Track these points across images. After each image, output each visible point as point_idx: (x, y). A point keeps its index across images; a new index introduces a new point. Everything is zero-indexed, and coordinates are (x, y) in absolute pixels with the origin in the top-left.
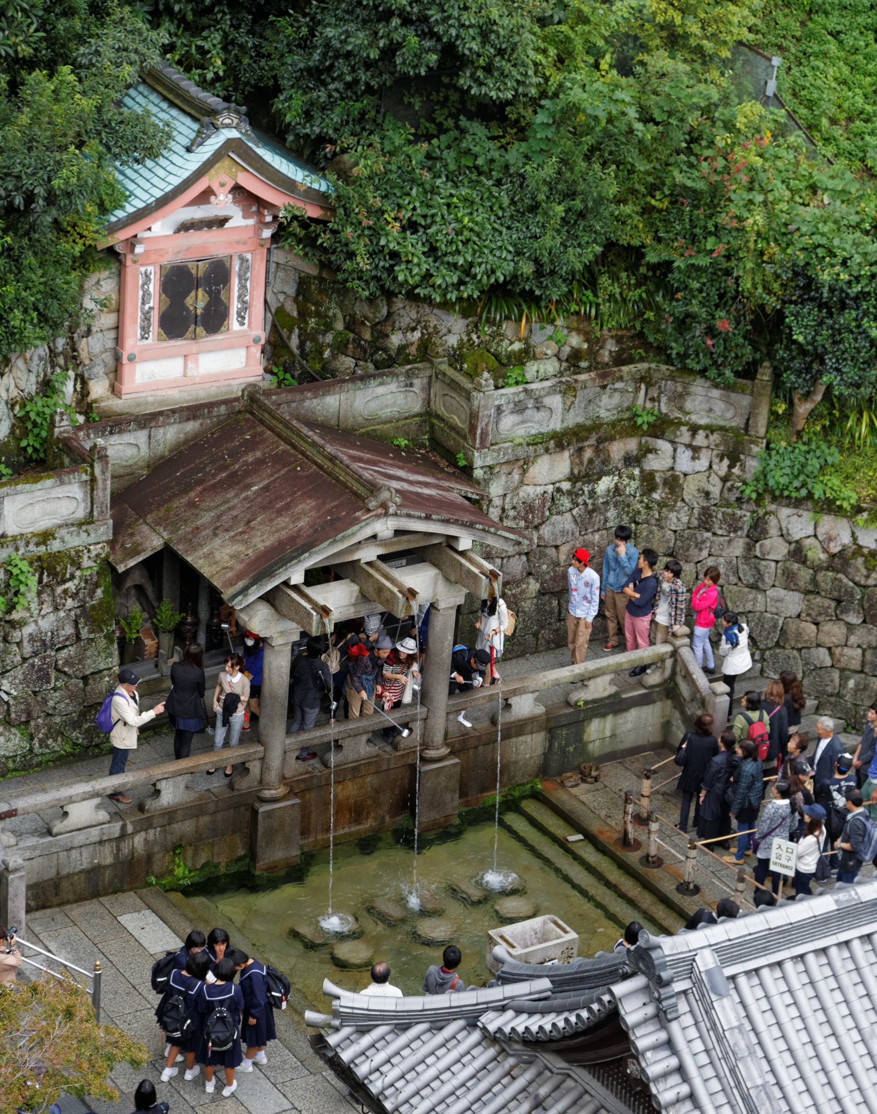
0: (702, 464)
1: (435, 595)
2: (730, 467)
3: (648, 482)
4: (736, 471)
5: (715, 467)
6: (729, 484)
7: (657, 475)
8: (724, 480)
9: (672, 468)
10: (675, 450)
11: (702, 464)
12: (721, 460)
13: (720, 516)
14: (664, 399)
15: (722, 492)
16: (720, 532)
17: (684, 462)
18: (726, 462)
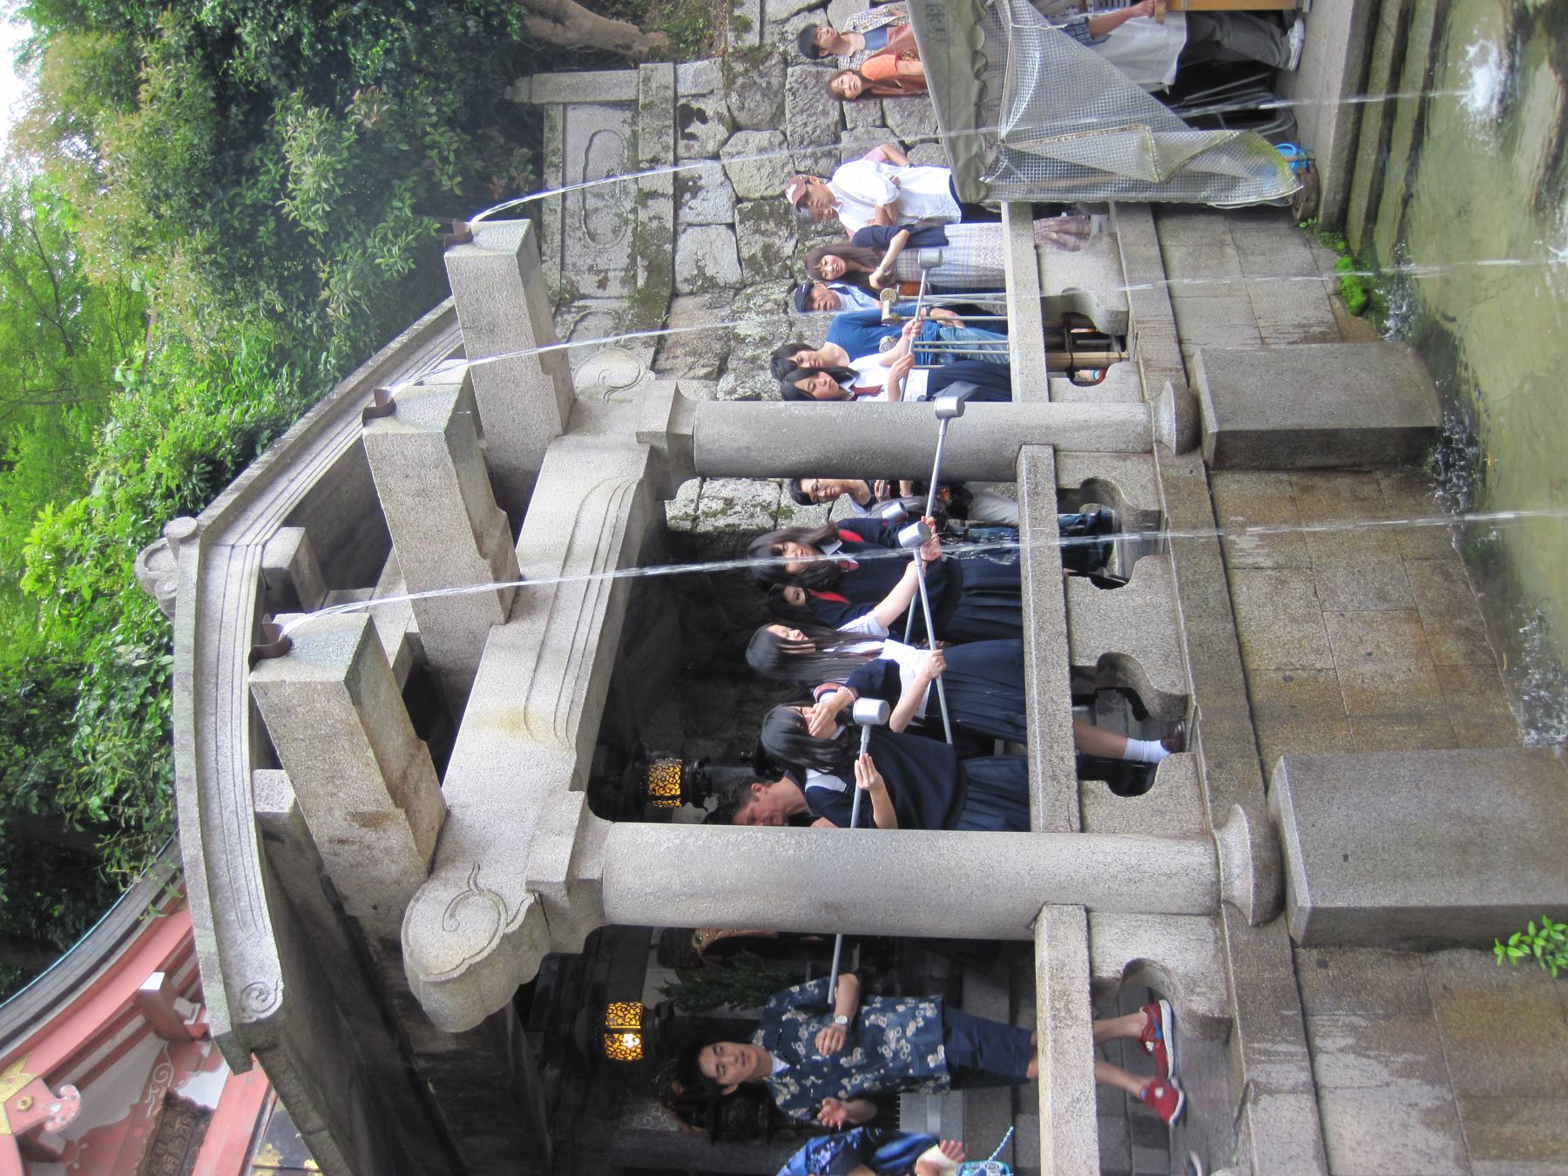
0: (707, 171)
1: (627, 447)
2: (702, 117)
3: (761, 266)
4: (710, 107)
5: (711, 147)
6: (742, 118)
7: (746, 254)
8: (735, 127)
9: (731, 226)
10: (690, 225)
11: (707, 171)
12: (692, 137)
13: (800, 120)
14: (602, 263)
15: (757, 128)
16: (835, 115)
17: (713, 204)
18: (695, 128)
